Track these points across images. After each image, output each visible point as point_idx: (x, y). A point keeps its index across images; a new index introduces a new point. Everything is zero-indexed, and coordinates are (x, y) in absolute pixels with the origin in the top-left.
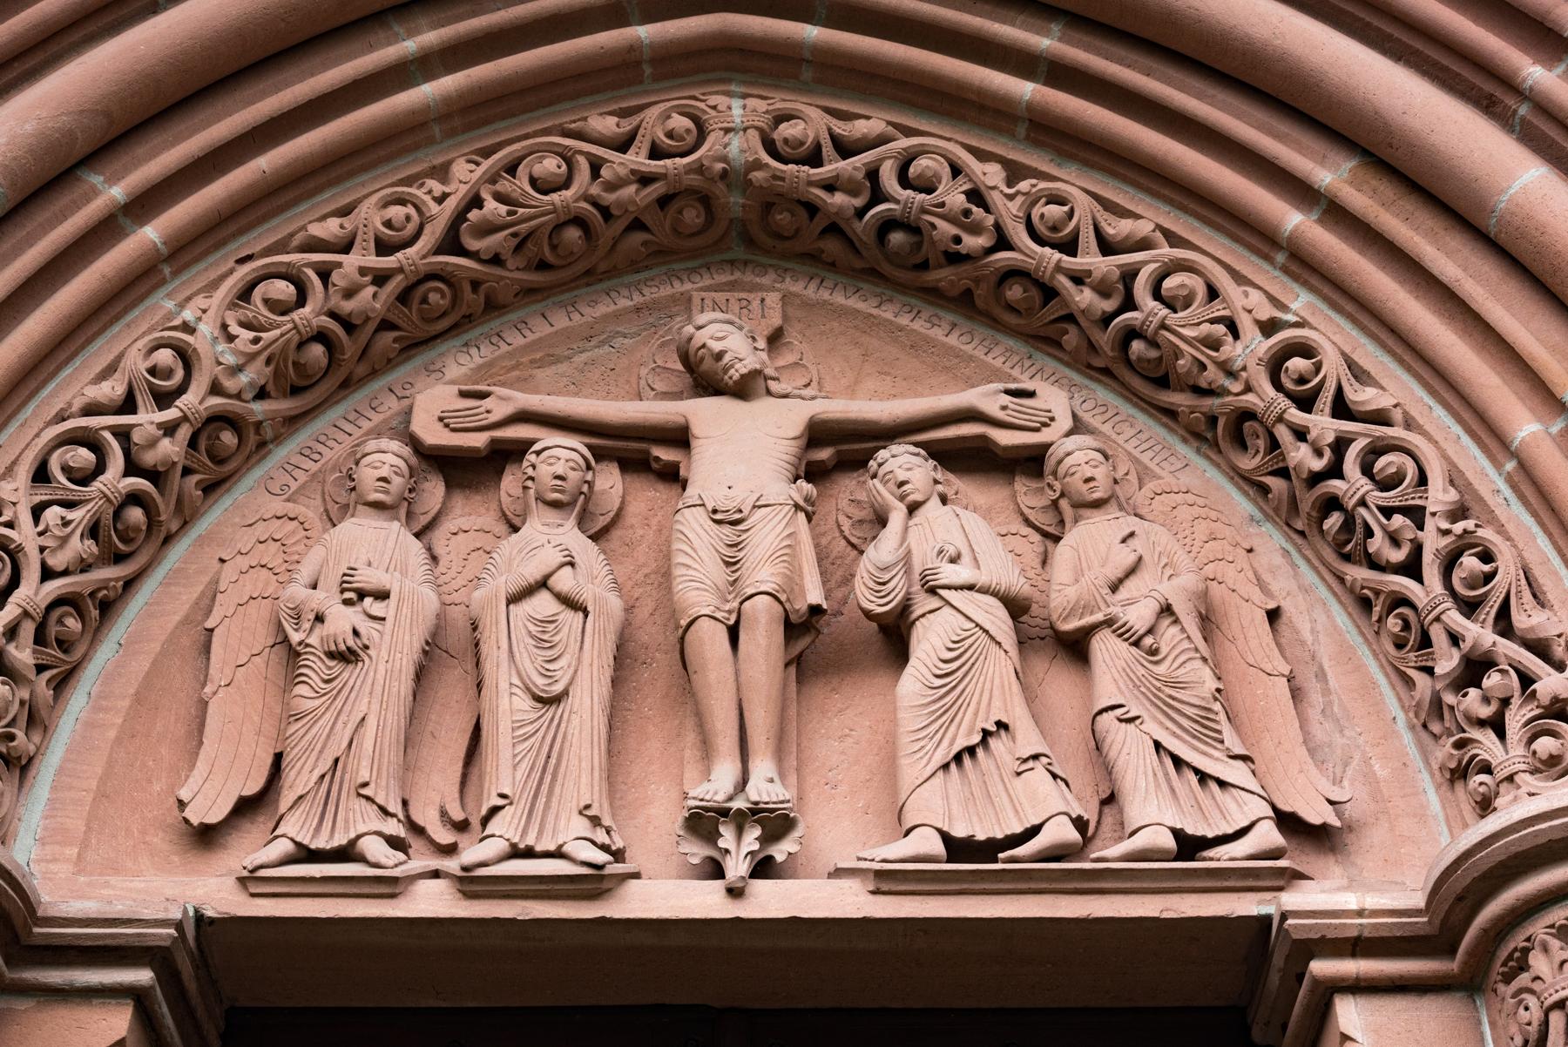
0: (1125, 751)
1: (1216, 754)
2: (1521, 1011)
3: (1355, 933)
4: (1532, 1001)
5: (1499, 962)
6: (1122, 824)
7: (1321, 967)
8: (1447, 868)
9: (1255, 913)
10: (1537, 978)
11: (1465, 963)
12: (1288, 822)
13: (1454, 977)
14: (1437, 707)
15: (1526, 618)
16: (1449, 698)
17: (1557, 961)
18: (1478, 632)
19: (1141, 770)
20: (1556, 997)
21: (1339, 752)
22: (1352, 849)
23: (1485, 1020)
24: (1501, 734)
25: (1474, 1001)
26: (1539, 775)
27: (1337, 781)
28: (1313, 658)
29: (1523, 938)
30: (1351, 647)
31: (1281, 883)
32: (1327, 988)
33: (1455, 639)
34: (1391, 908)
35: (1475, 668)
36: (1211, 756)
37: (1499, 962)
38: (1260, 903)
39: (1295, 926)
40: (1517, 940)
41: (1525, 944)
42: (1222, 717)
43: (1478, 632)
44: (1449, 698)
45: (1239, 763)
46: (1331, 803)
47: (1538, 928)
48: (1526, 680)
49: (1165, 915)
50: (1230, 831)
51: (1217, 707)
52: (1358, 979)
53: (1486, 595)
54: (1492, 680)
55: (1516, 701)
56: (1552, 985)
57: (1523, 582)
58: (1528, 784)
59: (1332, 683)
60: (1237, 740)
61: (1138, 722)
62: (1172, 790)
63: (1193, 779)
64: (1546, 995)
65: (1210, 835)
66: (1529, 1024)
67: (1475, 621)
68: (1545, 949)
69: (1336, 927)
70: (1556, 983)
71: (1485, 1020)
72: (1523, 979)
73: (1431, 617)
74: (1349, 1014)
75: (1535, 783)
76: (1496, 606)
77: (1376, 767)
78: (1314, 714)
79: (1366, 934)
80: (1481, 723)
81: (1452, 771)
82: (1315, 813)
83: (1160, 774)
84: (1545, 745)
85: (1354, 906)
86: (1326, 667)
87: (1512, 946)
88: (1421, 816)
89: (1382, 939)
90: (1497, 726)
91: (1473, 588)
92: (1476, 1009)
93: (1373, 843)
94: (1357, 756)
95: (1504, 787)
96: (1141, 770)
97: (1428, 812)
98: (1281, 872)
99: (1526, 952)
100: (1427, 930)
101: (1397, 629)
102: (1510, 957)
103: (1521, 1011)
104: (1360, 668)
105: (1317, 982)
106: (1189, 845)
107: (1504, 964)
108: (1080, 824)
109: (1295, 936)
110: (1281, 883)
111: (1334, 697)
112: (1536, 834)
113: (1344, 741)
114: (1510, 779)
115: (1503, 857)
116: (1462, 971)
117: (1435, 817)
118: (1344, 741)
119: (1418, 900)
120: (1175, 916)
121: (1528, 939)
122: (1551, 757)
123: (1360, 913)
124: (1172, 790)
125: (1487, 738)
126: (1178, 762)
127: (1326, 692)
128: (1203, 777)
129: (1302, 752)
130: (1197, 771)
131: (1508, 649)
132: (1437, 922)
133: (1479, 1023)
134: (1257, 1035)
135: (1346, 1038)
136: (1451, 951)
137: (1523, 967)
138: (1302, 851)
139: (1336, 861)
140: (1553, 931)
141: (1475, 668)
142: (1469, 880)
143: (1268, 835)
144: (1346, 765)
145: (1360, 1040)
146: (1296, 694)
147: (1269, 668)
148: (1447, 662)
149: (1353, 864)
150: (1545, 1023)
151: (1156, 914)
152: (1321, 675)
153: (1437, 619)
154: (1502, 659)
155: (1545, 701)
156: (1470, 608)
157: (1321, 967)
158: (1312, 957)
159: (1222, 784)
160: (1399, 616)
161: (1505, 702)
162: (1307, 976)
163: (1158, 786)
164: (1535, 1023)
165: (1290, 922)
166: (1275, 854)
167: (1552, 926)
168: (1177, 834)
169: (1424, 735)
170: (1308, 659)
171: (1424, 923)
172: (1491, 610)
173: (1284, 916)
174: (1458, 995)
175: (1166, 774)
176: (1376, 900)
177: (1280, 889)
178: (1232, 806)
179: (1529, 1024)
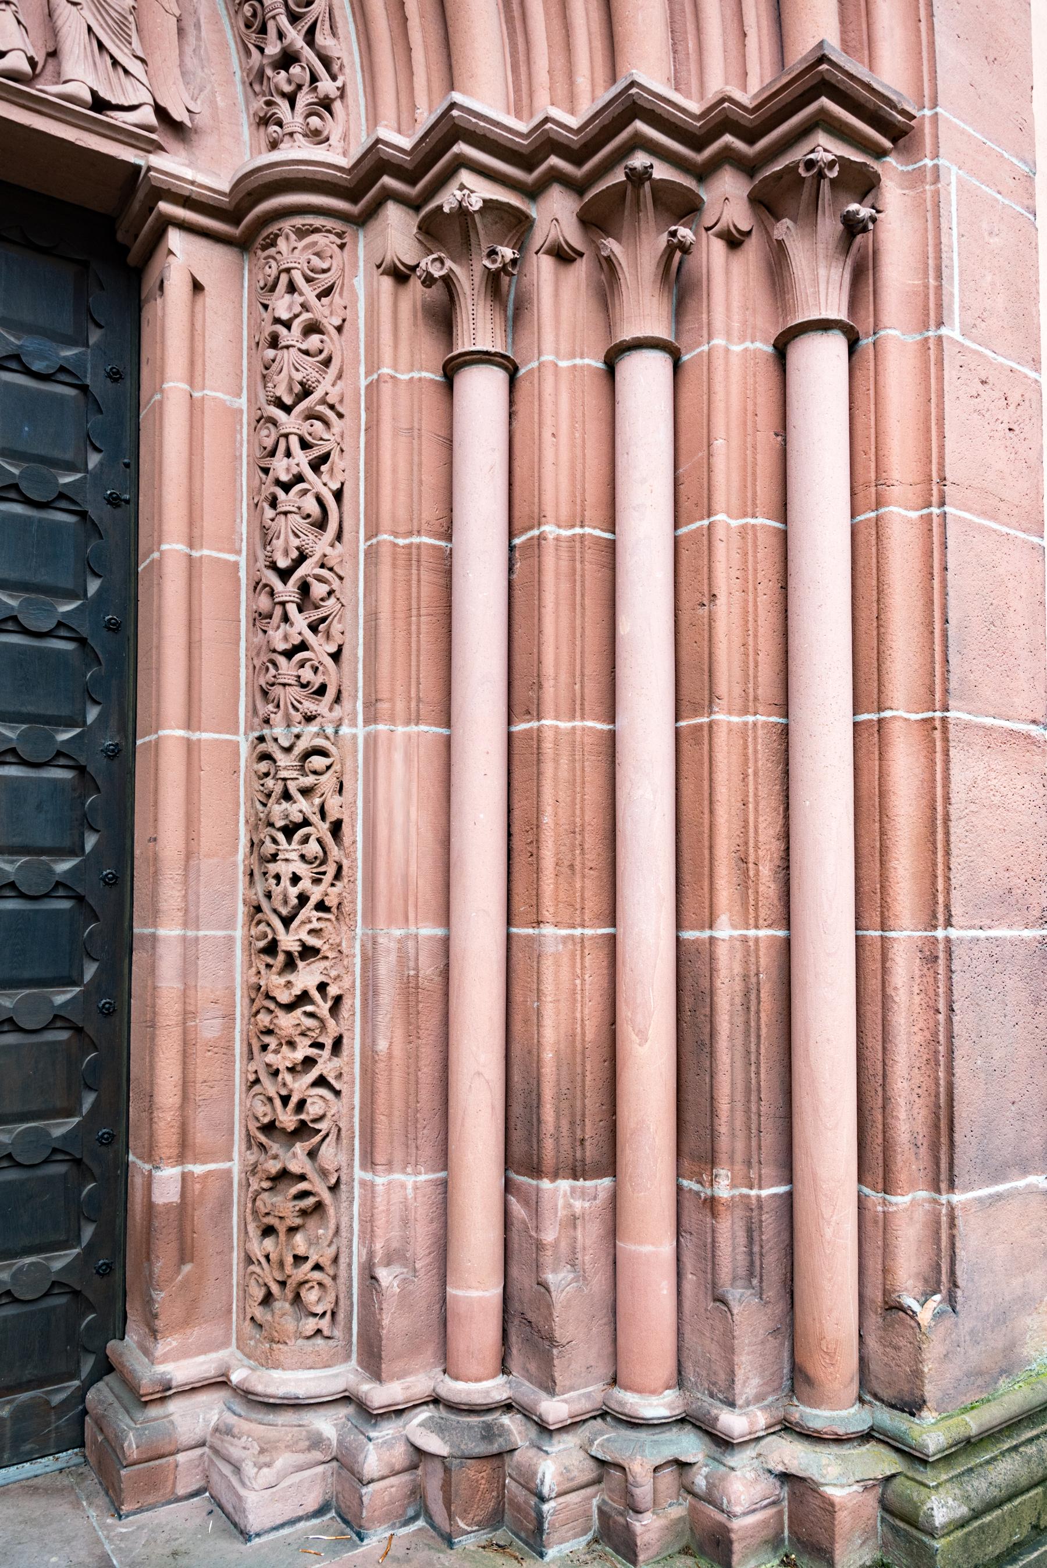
0: (68, 24)
1: (126, 50)
2: (267, 268)
3: (187, 194)
4: (273, 264)
6: (59, 74)
7: (165, 207)
10: (279, 252)
11: (243, 232)
12: (161, 112)
13: (235, 238)
14: (261, 75)
15: (322, 39)
16: (269, 72)
17: (292, 246)
18: (295, 37)
19: (77, 41)
20: (287, 266)
21: (199, 80)
22: (195, 144)
23: (246, 267)
24: (292, 106)
27: (194, 99)
28: (195, 12)
30: (218, 14)
33: (281, 35)
35: (287, 59)
36: (122, 51)
37: (261, 237)
38: (136, 156)
39: (155, 177)
40: (273, 228)
42: (133, 27)
43: (295, 37)
44: (269, 72)
45: (139, 62)
46: (189, 111)
47: (287, 225)
48: (314, 79)
49: (78, 143)
50: (126, 104)
51: (131, 18)
52: (184, 221)
53: (305, 14)
54: (296, 70)
55: (305, 89)
57: (327, 15)
59: (203, 34)
60: (139, 46)
61: (79, 7)
62: (95, 63)
63: (109, 62)
65: (114, 102)
67: (295, 28)
68: (287, 238)
69: (178, 186)
71: (246, 267)
72: (272, 251)
73: (270, 14)
74: (175, 239)
76: (309, 24)
77: (218, 99)
78: (189, 50)
79: (194, 196)
80: (283, 95)
81: (261, 118)
82: (178, 114)
83: (88, 49)
84: (314, 121)
85: (190, 177)
86: (202, 21)
87: (270, 230)
88: (237, 138)
89: (202, 202)
90: (291, 99)
91: (299, 6)
93: (207, 143)
94: (209, 87)
95: (287, 138)
96: (77, 41)
99: (277, 236)
101: (249, 14)
102: (268, 237)
103: (267, 268)
104: (221, 31)
106: (100, 104)
107: (264, 240)
108: (32, 62)
111: (202, 44)
113: (203, 75)
114: (291, 134)
116: (240, 237)
118: (203, 75)
119: (226, 187)
120: (84, 145)
121: (280, 230)
122: (316, 130)
123: (193, 183)
124: (95, 63)
125: (284, 104)
126: (101, 46)
127: (199, 38)
128: (115, 63)
129: (177, 71)
130: (112, 57)
131: (308, 53)
132: (233, 204)
133: (243, 268)
134: (120, 236)
135: (170, 252)
137: (273, 244)
141: (287, 59)
142: (256, 185)
143: (147, 116)
144: (201, 91)
146: (181, 31)
147: (167, 6)
148: (273, 49)
149: (193, 153)
150: (278, 278)
151: (72, 140)
152: (198, 26)
153: (274, 17)
154: (304, 59)
155: (321, 96)
156: (294, 18)
157: (165, 207)
158: (160, 199)
159: (126, 72)
160: (252, 6)
161: (300, 87)
163: (86, 56)
164: (273, 276)
165: (152, 173)
166: (150, 129)
167: (294, 227)
168: (94, 93)
169: (249, 89)
170: (192, 11)
172: (305, 25)
173: (149, 169)
174: (236, 249)
175: (92, 51)
177: (149, 152)
178: (130, 89)
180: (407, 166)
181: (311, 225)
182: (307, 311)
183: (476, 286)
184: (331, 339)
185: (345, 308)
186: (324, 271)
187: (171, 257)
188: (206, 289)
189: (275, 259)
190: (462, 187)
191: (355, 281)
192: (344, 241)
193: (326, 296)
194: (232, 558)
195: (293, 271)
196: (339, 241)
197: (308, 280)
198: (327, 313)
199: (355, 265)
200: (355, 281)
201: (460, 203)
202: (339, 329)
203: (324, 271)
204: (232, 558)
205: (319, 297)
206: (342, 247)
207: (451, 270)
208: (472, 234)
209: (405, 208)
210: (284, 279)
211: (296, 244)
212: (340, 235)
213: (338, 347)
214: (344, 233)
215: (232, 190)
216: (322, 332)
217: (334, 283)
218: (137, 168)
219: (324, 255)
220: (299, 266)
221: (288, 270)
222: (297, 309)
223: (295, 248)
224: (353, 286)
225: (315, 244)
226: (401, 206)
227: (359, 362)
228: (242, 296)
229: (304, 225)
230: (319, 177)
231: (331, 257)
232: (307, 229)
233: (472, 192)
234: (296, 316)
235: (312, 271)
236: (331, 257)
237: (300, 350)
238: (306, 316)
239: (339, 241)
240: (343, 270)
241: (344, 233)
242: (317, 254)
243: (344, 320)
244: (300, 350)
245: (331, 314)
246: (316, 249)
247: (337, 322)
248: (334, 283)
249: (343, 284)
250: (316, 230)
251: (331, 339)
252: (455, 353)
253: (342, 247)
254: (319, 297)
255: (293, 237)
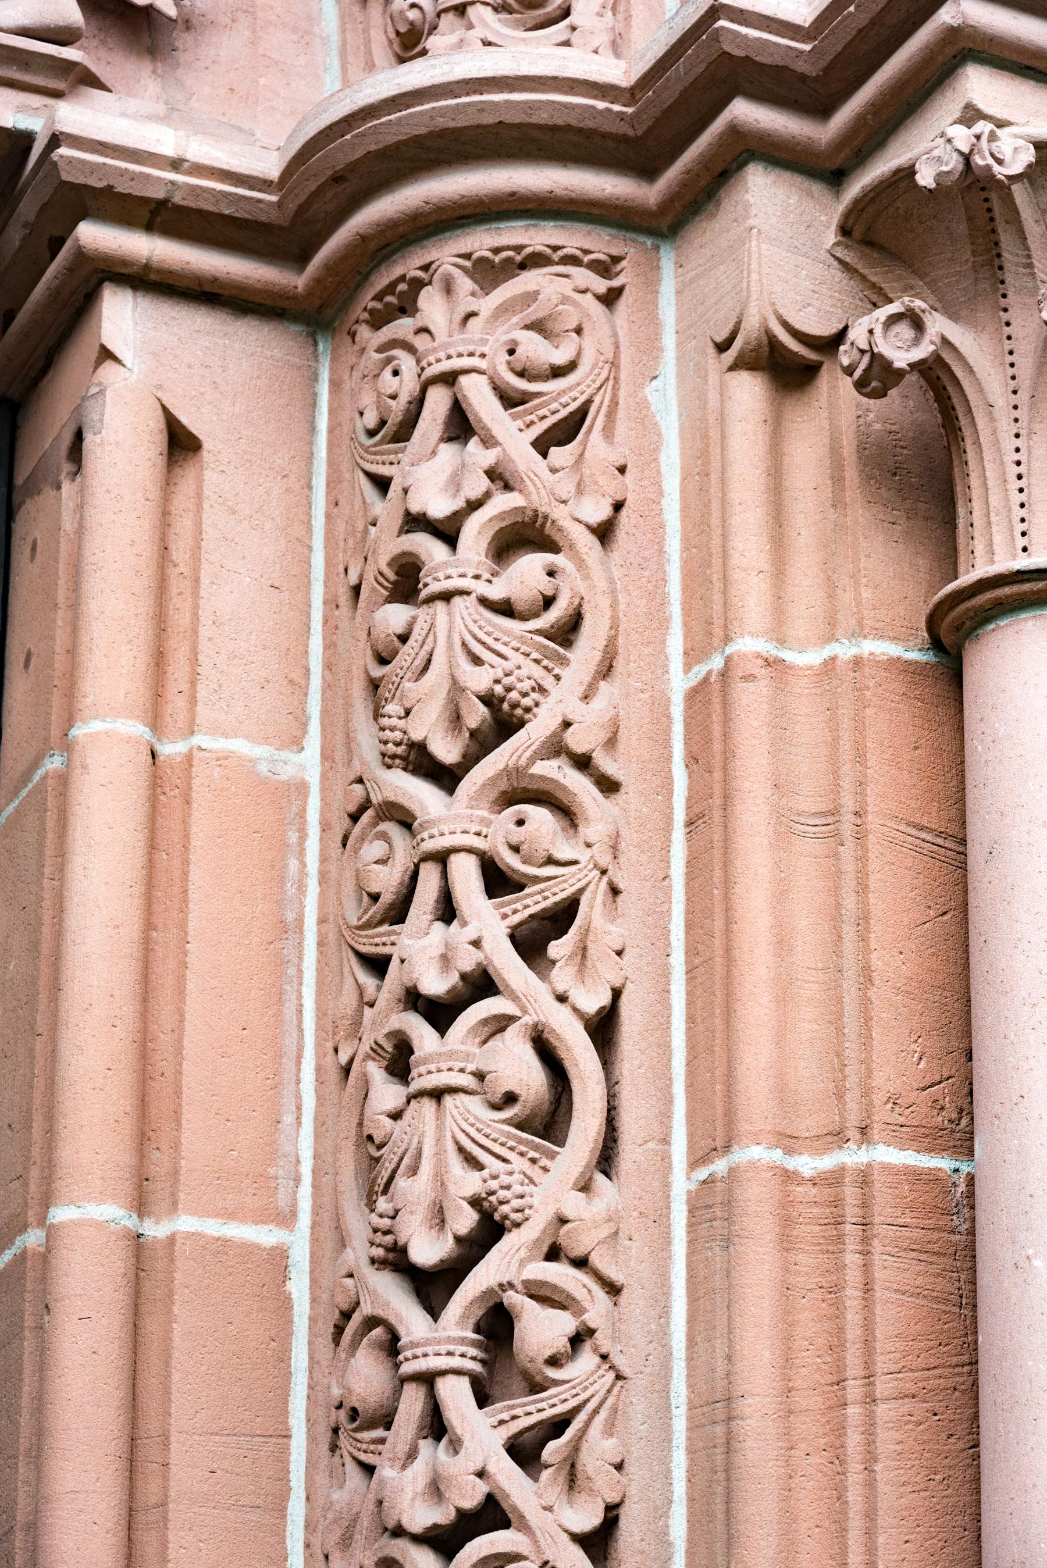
2: (387, 374)
3: (160, 195)
4: (406, 362)
5: (372, 292)
8: (330, 127)
9: (9, 124)
11: (317, 281)
13: (295, 298)
20: (446, 366)
22: (183, 57)
23: (325, 375)
25: (316, 344)
26: (505, 16)
29: (419, 262)
31: (60, 85)
32: (96, 271)
34: (225, 167)
37: (372, 292)
38: (20, 109)
39: (70, 161)
40: (409, 265)
41: (420, 274)
52: (147, 267)
56: (446, 346)
58: (486, 25)
64: (432, 359)
66: (394, 397)
68: (448, 288)
69: (134, 177)
70: (449, 345)
71: (325, 375)
72: (402, 328)
75: (498, 26)
79: (177, 199)
85: (168, 149)
87: (398, 271)
92: (316, 356)
97: (316, 30)
98: (68, 66)
99: (418, 285)
100: (273, 217)
102: (391, 288)
103: (387, 374)
105: (82, 256)
107: (379, 297)
109: (65, 177)
110: (60, 85)
112: (482, 107)
115: (423, 130)
117: (325, 41)
119: (271, 167)
121: (426, 268)
123: (176, 164)
132: (292, 206)
133: (315, 378)
135: (106, 355)
136: (300, 259)
137: (407, 307)
138: (103, 42)
139: (154, 72)
140: (467, 264)
142: (359, 154)
145: (129, 364)
149: (179, 83)
150: (419, 402)
162: (68, 244)
164: (404, 398)
165: (63, 151)
166: (62, 36)
167: (467, 256)
171: (270, 204)
173: (55, 140)
174: (295, 328)
176: (206, 148)
177: (57, 95)
179: (394, 397)
180: (801, 67)
181: (519, 249)
182: (507, 487)
183: (1025, 381)
184: (580, 563)
185: (622, 470)
186: (558, 372)
187: (108, 368)
188: (206, 445)
189: (410, 349)
190: (971, 115)
191: (651, 392)
192: (616, 283)
193: (561, 443)
194: (266, 1236)
195: (463, 380)
196: (601, 285)
197: (510, 400)
198: (565, 486)
199: (651, 347)
200: (651, 392)
201: (967, 158)
202: (604, 533)
203: (558, 372)
204: (266, 1236)
205: (542, 445)
206: (610, 299)
207: (945, 341)
208: (1007, 240)
209: (798, 179)
210: (438, 401)
211: (473, 304)
212: (604, 268)
213: (602, 585)
214: (616, 260)
215: (287, 173)
216: (551, 546)
217: (589, 402)
218: (23, 140)
219: (558, 327)
220: (482, 364)
221: (449, 379)
222: (477, 485)
223: (472, 314)
224: (644, 405)
225: (532, 297)
226: (787, 175)
227: (664, 623)
228: (310, 457)
229: (496, 251)
230: (542, 118)
231: (579, 331)
232: (508, 260)
233: (1001, 124)
234: (473, 506)
235: (521, 374)
236: (579, 331)
237: (484, 602)
238: (502, 503)
239: (601, 285)
240: (614, 364)
241: (616, 260)
242: (538, 326)
243: (618, 506)
244: (484, 601)
245: (580, 489)
246: (534, 312)
247: (598, 512)
248: (589, 402)
249: (614, 403)
250: (536, 260)
251: (580, 563)
252: (965, 579)
253: (610, 299)
254: (542, 445)
255: (465, 284)
